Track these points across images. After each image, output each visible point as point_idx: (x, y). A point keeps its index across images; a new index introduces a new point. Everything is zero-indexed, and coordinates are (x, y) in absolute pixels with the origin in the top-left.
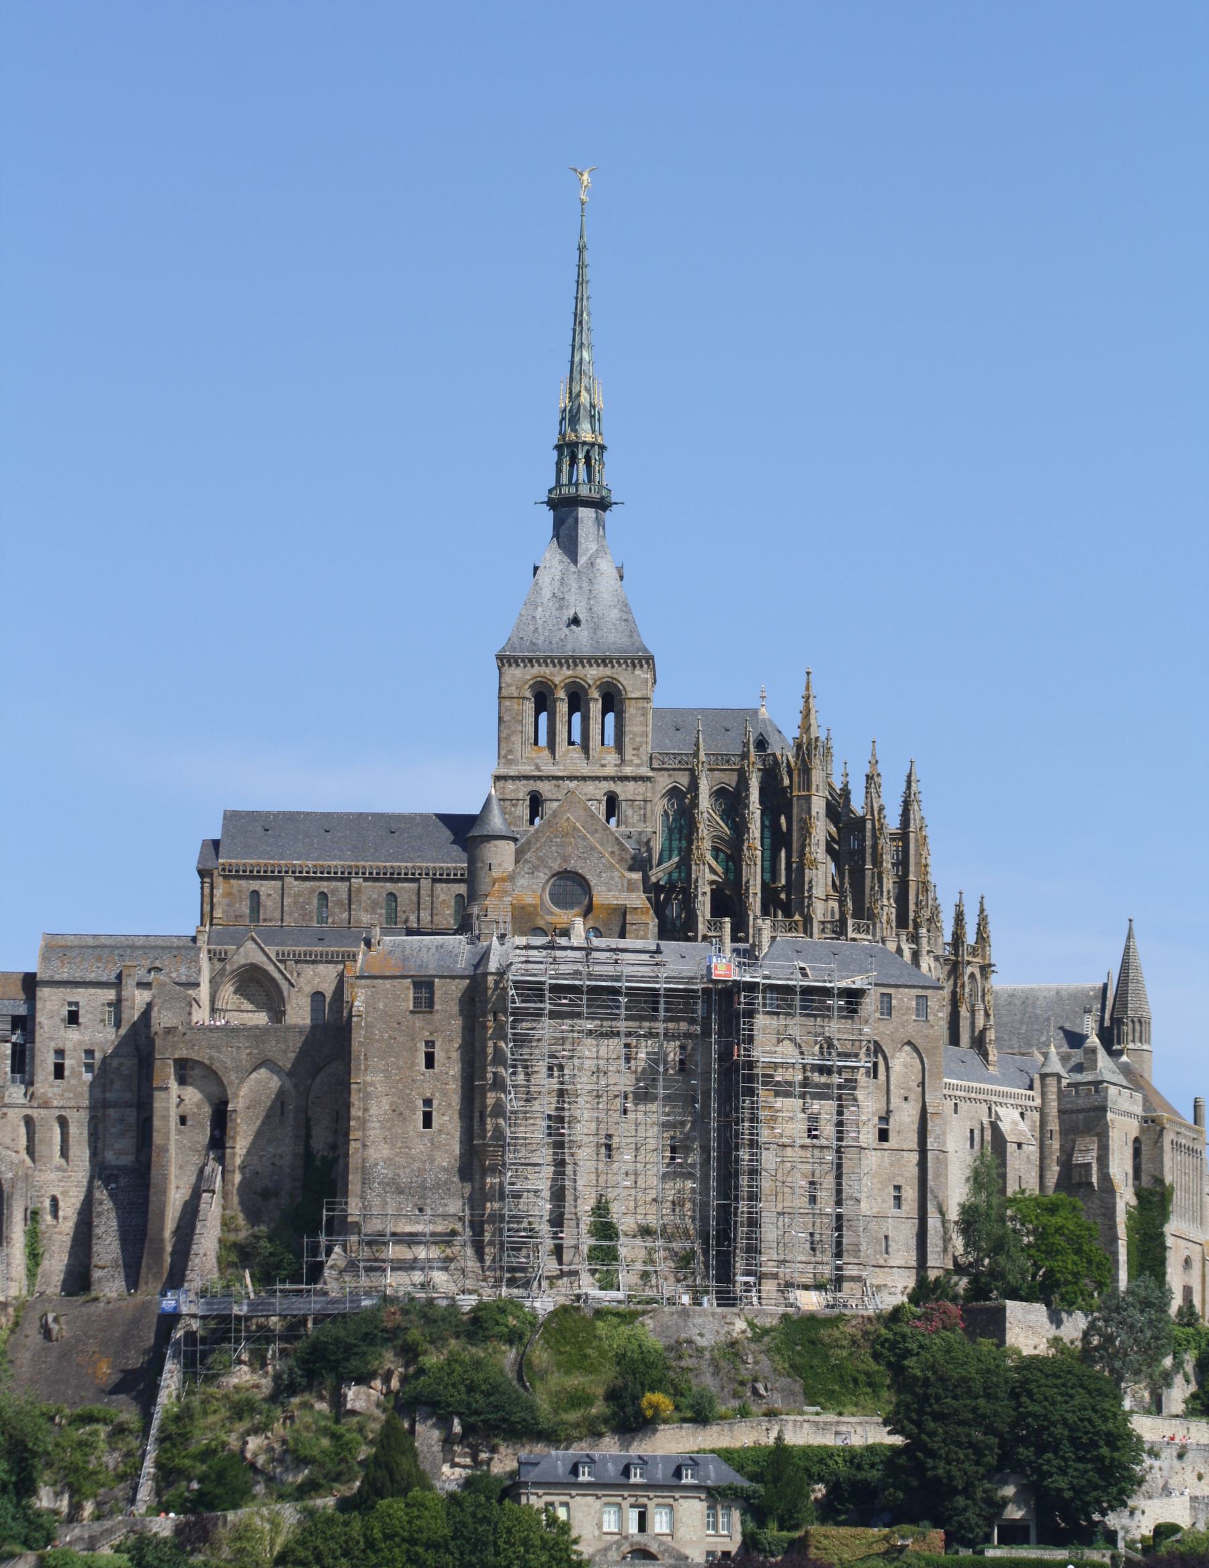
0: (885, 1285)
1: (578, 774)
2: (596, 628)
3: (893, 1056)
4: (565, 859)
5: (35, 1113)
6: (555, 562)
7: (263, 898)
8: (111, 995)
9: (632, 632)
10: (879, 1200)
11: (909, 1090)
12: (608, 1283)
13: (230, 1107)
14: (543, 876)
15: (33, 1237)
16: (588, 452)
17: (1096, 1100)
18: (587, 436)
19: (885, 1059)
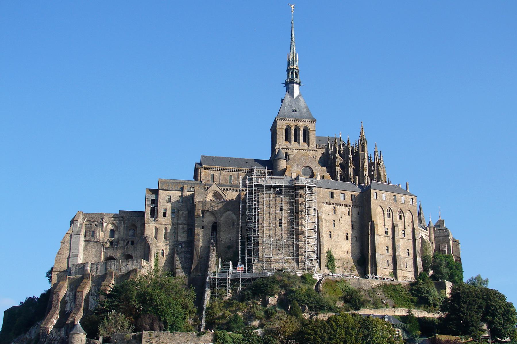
0: (407, 276)
1: (298, 149)
2: (301, 113)
3: (405, 214)
4: (306, 163)
5: (158, 226)
6: (288, 97)
7: (215, 176)
8: (180, 193)
9: (310, 114)
10: (404, 253)
11: (409, 223)
12: (333, 271)
13: (218, 223)
14: (300, 167)
15: (157, 260)
16: (296, 71)
17: (446, 234)
18: (295, 67)
19: (403, 214)
